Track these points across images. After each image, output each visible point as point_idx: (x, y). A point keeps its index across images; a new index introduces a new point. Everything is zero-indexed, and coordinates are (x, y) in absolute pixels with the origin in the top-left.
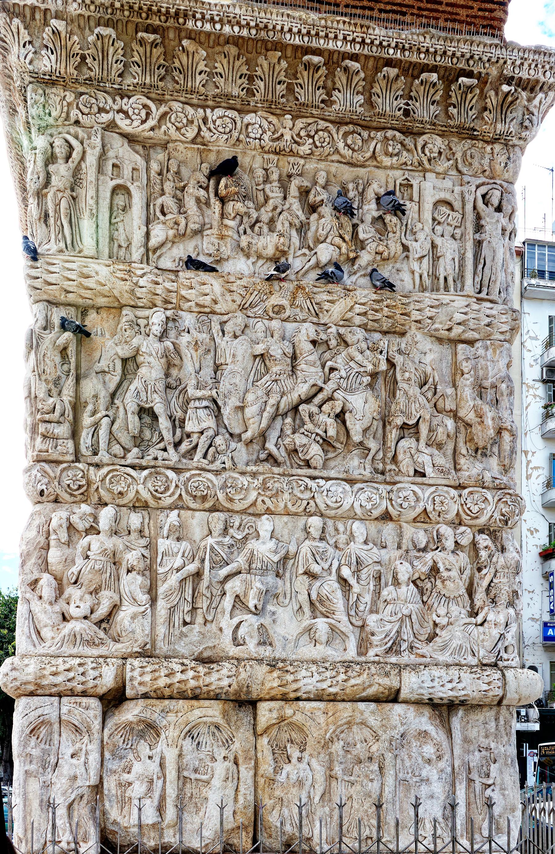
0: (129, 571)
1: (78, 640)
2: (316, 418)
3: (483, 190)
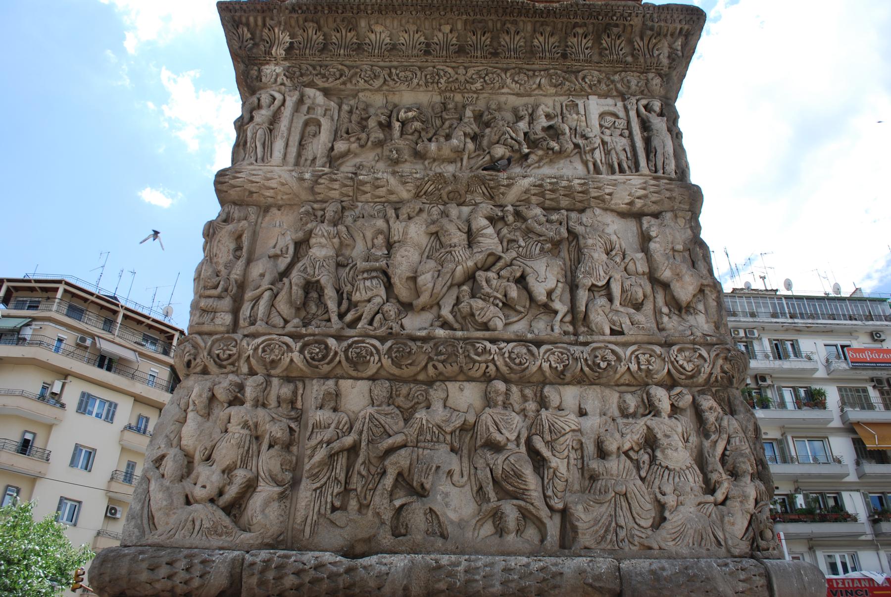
0: (271, 446)
1: (197, 528)
2: (494, 282)
3: (644, 102)
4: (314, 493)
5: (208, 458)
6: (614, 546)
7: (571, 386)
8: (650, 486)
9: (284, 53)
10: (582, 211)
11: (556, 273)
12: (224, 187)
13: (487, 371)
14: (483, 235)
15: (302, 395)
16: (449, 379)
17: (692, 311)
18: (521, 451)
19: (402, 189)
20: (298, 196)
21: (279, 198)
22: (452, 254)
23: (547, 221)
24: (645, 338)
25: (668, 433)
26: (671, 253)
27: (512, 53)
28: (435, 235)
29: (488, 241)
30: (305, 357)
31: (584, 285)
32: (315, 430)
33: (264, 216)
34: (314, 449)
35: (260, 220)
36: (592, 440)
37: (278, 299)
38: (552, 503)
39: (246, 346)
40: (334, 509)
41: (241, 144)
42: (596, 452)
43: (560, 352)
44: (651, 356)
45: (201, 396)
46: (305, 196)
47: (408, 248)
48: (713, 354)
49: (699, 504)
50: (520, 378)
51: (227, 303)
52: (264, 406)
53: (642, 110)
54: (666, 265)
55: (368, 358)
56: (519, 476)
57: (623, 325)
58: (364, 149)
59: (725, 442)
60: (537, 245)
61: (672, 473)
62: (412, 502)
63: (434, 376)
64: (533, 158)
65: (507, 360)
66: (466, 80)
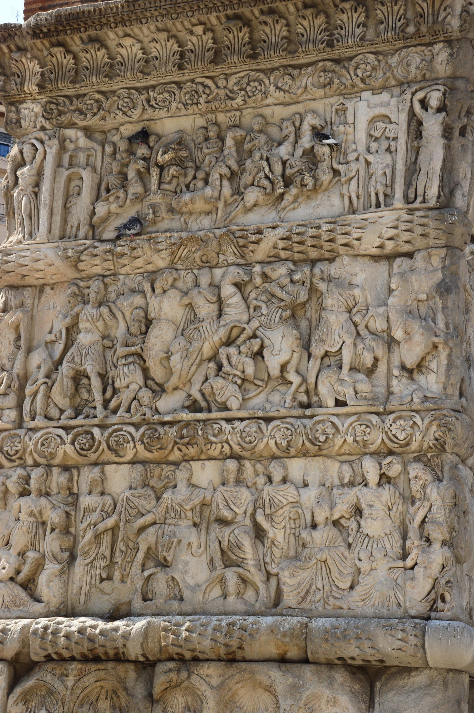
0: (53, 530)
2: (234, 359)
3: (420, 95)
5: (8, 543)
9: (37, 88)
10: (331, 260)
17: (424, 370)
20: (65, 276)
24: (365, 409)
25: (372, 503)
26: (415, 303)
27: (272, 52)
33: (40, 298)
38: (269, 568)
39: (28, 442)
40: (102, 580)
46: (71, 274)
48: (427, 421)
49: (390, 569)
52: (48, 494)
53: (417, 107)
58: (124, 208)
59: (426, 510)
61: (371, 541)
64: (289, 198)
65: (239, 439)
66: (227, 95)
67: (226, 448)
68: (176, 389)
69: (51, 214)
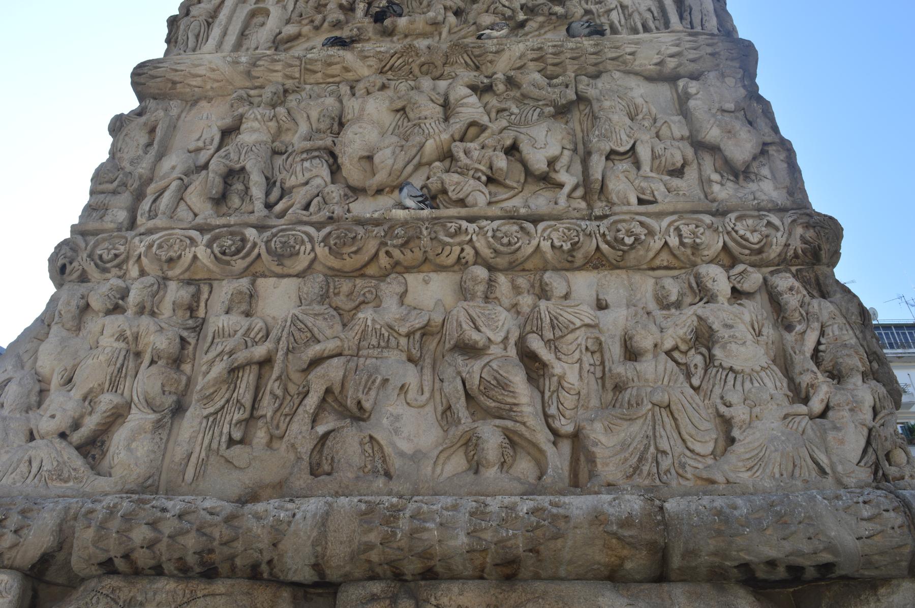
1: (34, 470)
2: (476, 154)
4: (205, 421)
6: (653, 480)
7: (583, 273)
8: (708, 396)
10: (597, 76)
11: (560, 137)
12: (142, 80)
13: (462, 255)
14: (462, 105)
15: (207, 300)
16: (409, 269)
17: (753, 177)
18: (509, 354)
19: (361, 64)
20: (231, 83)
21: (208, 87)
22: (420, 127)
23: (549, 85)
24: (688, 206)
25: (730, 322)
28: (402, 112)
29: (470, 110)
30: (213, 252)
31: (599, 149)
32: (216, 341)
33: (190, 110)
34: (212, 363)
35: (183, 115)
36: (617, 339)
37: (189, 190)
38: (556, 424)
40: (231, 442)
41: (173, 40)
42: (622, 354)
43: (565, 228)
44: (697, 227)
45: (68, 303)
46: (240, 81)
47: (364, 125)
49: (786, 417)
50: (510, 263)
51: (125, 198)
52: (153, 314)
54: (711, 122)
55: (297, 247)
56: (503, 385)
57: (656, 193)
60: (535, 110)
62: (343, 427)
63: (388, 267)
64: (532, 25)
65: (491, 239)
67: (469, 252)
68: (379, 191)
69: (225, 34)
